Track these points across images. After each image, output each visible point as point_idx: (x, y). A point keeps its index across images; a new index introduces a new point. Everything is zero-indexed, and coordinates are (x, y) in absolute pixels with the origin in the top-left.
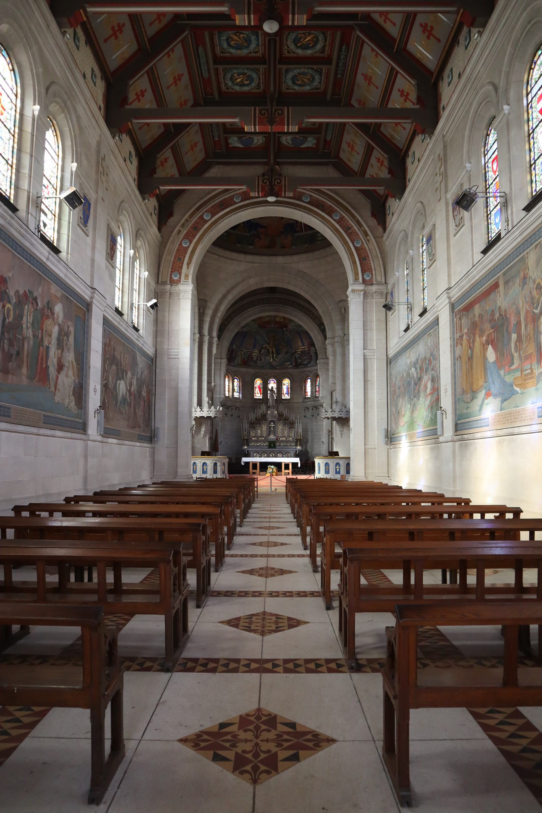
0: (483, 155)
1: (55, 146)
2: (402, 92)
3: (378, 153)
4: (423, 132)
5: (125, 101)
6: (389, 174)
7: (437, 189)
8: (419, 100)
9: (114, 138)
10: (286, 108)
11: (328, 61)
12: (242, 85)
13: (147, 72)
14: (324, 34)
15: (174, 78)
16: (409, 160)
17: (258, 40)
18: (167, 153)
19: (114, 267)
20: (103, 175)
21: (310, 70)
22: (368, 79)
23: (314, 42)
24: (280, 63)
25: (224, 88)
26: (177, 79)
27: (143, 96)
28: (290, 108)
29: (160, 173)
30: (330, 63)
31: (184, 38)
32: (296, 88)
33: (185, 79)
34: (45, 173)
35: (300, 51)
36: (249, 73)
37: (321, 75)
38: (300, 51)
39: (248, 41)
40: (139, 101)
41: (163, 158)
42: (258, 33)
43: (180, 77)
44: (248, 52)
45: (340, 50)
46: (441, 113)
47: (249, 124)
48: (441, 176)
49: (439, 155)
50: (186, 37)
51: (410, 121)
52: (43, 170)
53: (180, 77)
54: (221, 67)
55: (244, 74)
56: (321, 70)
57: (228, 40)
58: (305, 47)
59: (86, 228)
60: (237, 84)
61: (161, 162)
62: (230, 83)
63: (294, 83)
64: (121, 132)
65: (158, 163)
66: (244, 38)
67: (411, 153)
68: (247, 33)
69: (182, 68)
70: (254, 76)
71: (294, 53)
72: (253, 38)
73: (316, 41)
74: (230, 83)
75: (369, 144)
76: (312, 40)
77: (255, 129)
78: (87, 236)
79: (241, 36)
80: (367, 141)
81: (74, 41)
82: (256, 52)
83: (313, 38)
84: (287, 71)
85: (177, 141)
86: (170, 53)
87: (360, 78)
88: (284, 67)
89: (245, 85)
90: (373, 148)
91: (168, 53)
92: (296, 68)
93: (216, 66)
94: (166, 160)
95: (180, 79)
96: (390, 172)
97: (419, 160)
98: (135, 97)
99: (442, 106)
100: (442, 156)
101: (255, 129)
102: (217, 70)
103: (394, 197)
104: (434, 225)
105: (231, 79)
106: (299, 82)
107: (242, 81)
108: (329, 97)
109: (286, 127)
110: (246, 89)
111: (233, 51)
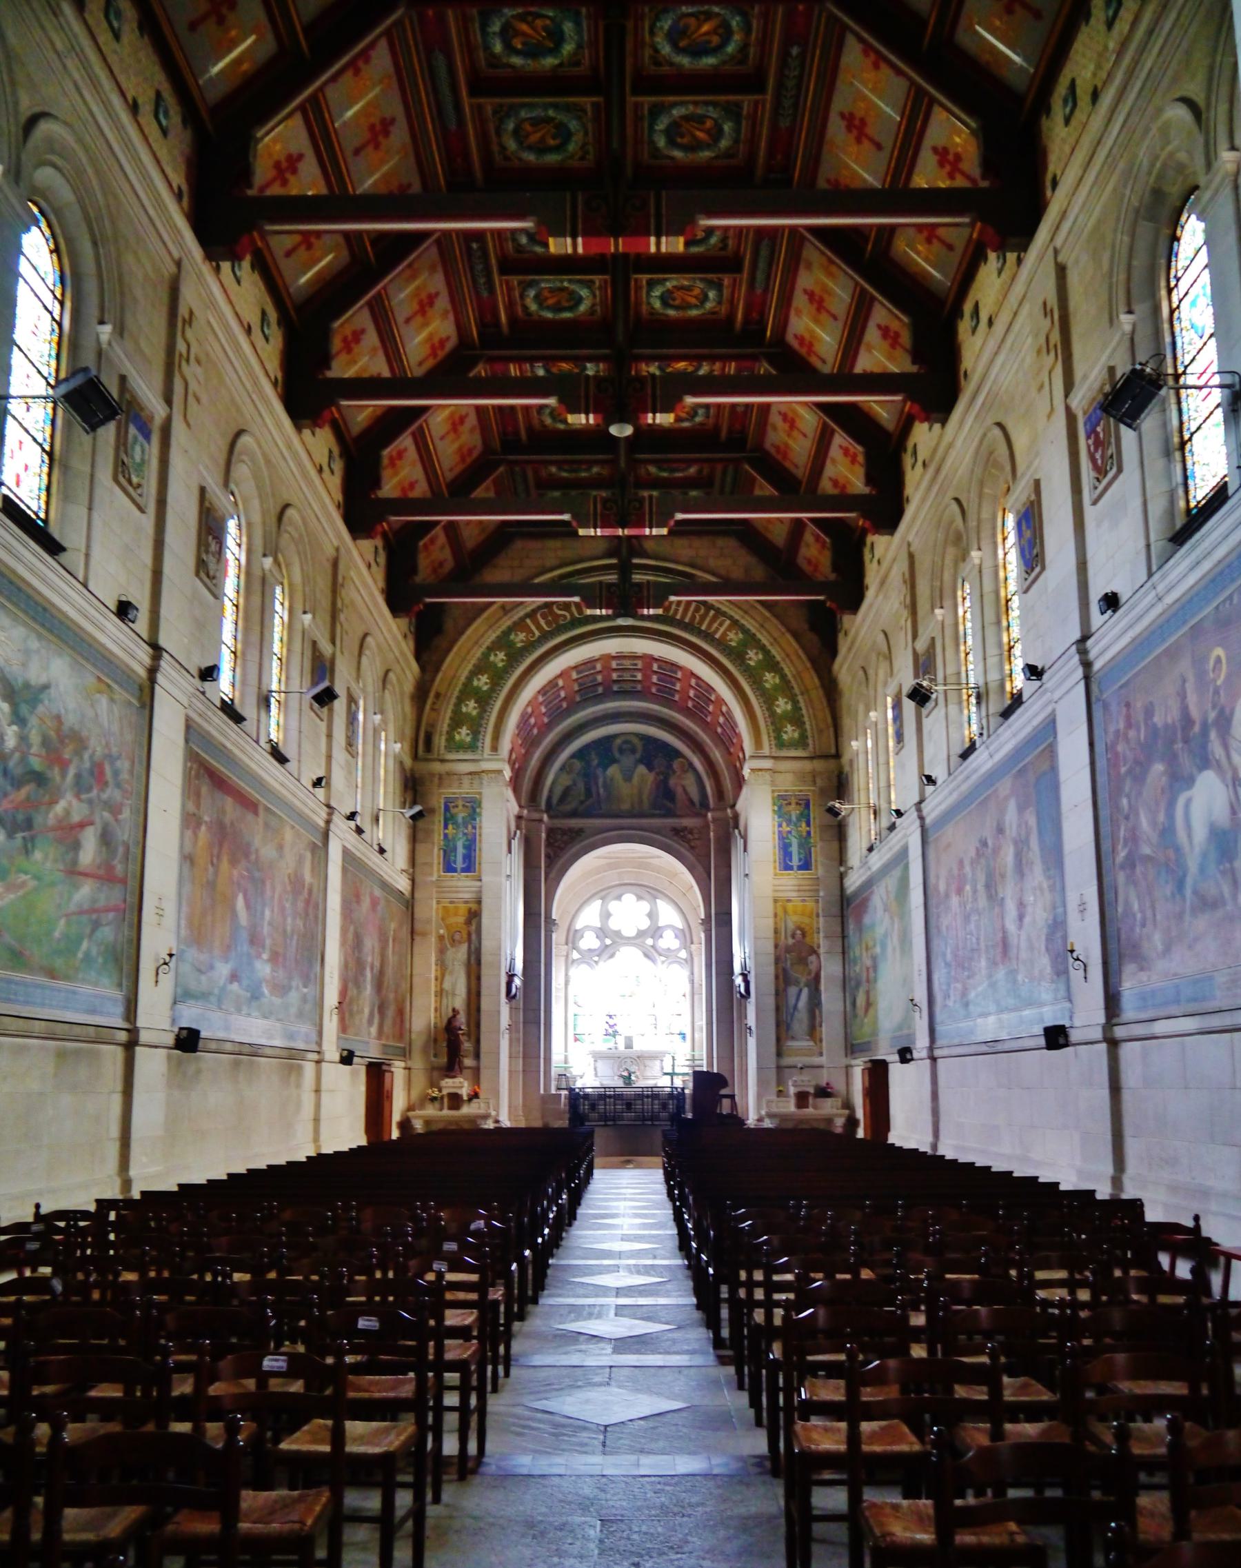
0: (1163, 293)
1: (51, 276)
2: (943, 155)
3: (883, 314)
4: (1001, 249)
5: (246, 174)
6: (914, 363)
7: (1041, 387)
8: (988, 165)
9: (217, 270)
10: (652, 194)
11: (755, 83)
12: (542, 149)
13: (302, 108)
14: (745, 15)
15: (372, 127)
16: (964, 326)
17: (579, 31)
18: (358, 317)
19: (217, 594)
20: (188, 361)
21: (711, 109)
22: (857, 126)
23: (720, 35)
24: (636, 91)
25: (498, 158)
26: (379, 130)
27: (294, 171)
28: (664, 193)
29: (341, 369)
30: (761, 89)
31: (395, 24)
32: (678, 154)
33: (400, 135)
34: (17, 336)
35: (685, 61)
36: (561, 117)
37: (738, 123)
38: (685, 61)
39: (557, 38)
40: (285, 183)
41: (348, 331)
42: (578, 13)
43: (386, 125)
44: (556, 62)
45: (785, 55)
46: (1049, 193)
47: (560, 233)
48: (1052, 354)
49: (1045, 304)
50: (398, 23)
51: (966, 220)
52: (11, 326)
53: (386, 125)
54: (489, 104)
55: (548, 120)
56: (738, 105)
57: (507, 33)
58: (698, 51)
59: (139, 491)
60: (530, 148)
61: (345, 340)
62: (512, 145)
63: (672, 142)
64: (235, 258)
65: (337, 344)
66: (545, 28)
67: (968, 308)
68: (551, 14)
69: (395, 108)
70: (573, 125)
71: (671, 64)
72: (568, 27)
73: (725, 33)
74: (512, 145)
75: (863, 290)
76: (714, 31)
77: (575, 245)
78: (142, 510)
79: (539, 23)
80: (857, 283)
81: (107, 16)
82: (578, 64)
83: (719, 26)
84: (657, 110)
85: (384, 288)
86: (361, 64)
87: (836, 128)
88: (648, 100)
89: (551, 150)
90: (873, 299)
91: (352, 64)
92: (674, 105)
93: (474, 101)
94: (357, 336)
95: (387, 134)
96: (916, 356)
97: (990, 322)
98: (271, 173)
99: (1049, 177)
100: (1053, 302)
101: (575, 245)
102: (480, 108)
103: (927, 418)
104: (1037, 483)
105: (516, 133)
106: (685, 141)
107: (543, 139)
108: (759, 172)
109: (653, 239)
110: (552, 158)
111: (517, 61)
